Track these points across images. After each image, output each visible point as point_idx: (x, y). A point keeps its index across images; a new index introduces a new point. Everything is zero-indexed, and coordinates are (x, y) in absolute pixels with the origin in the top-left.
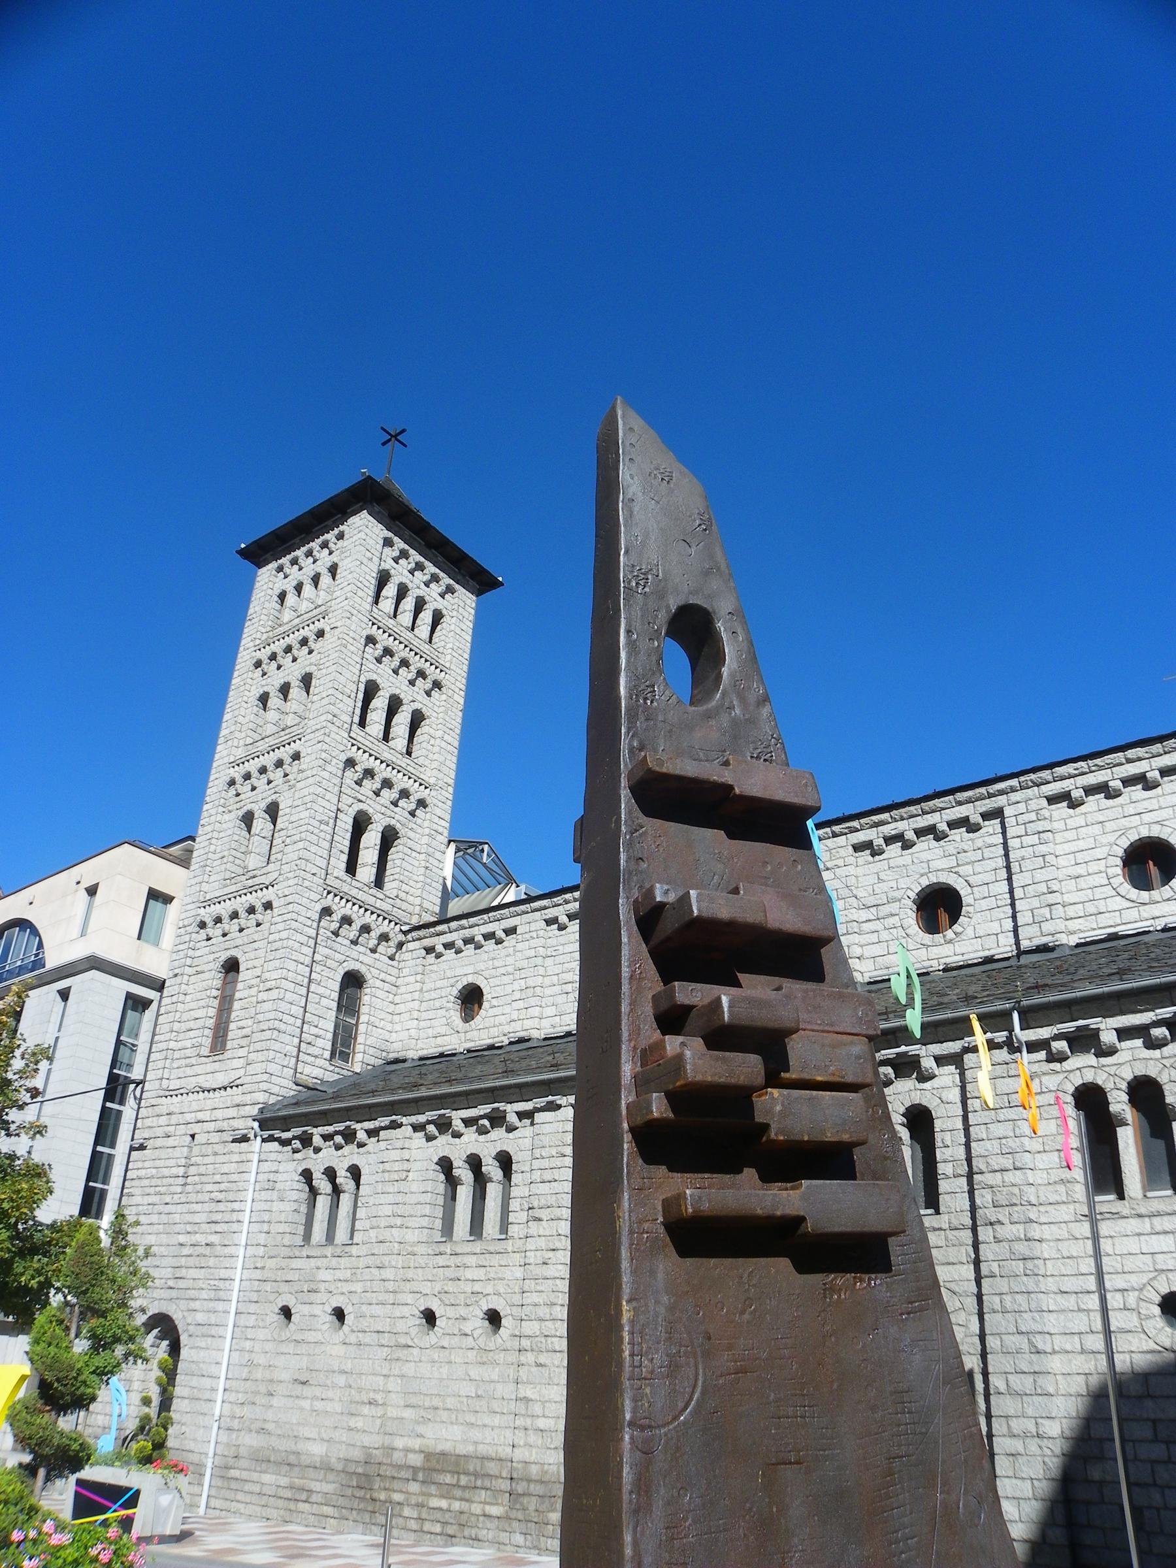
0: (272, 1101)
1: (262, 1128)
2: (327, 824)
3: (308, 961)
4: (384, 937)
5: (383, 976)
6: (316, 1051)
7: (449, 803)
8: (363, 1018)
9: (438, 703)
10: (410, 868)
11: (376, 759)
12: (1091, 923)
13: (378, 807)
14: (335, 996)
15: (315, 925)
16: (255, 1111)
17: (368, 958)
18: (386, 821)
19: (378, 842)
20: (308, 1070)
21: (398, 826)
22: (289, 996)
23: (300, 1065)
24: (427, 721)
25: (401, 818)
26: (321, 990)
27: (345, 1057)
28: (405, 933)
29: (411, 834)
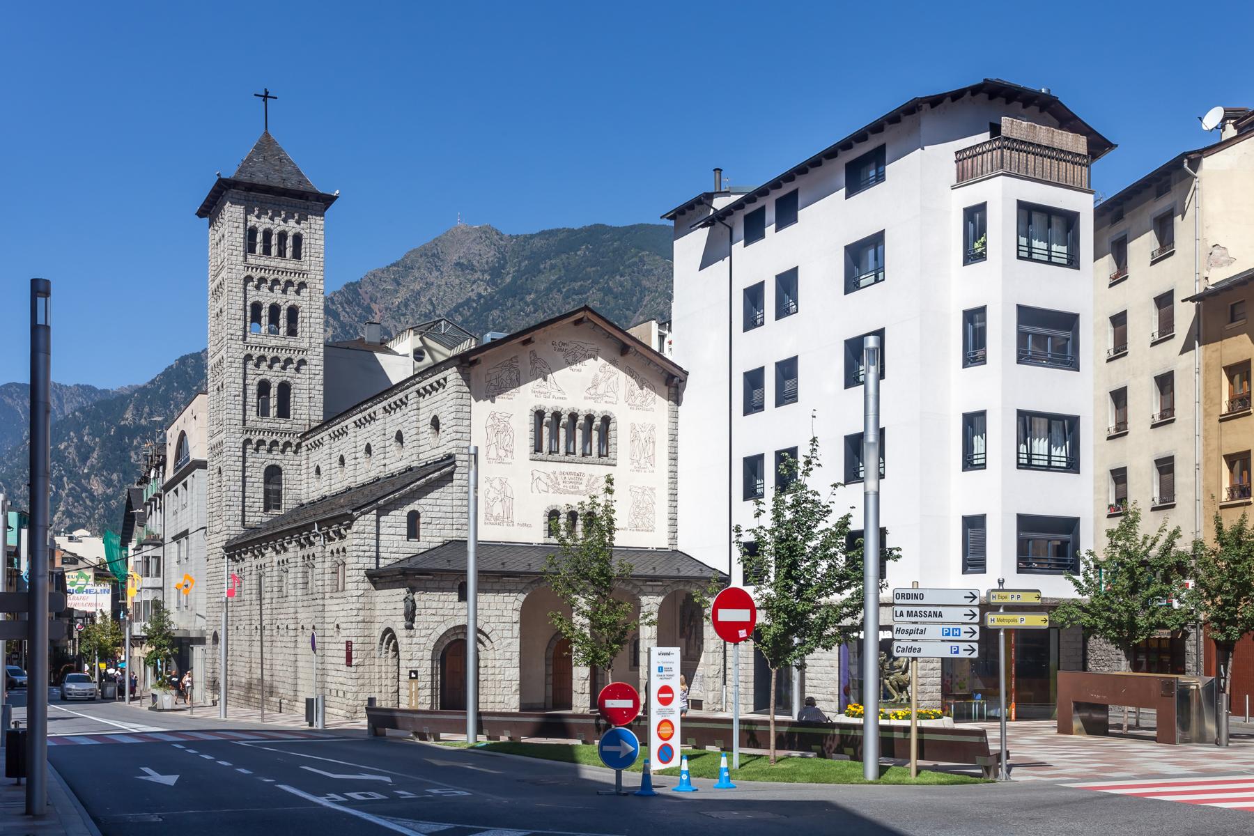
0: (232, 537)
1: (226, 552)
2: (239, 396)
3: (240, 468)
4: (288, 444)
5: (291, 462)
6: (255, 509)
7: (322, 354)
8: (284, 486)
9: (306, 295)
10: (300, 400)
11: (265, 348)
12: (435, 452)
13: (273, 374)
14: (262, 480)
15: (241, 450)
16: (224, 543)
17: (280, 456)
18: (279, 380)
19: (276, 393)
20: (251, 519)
21: (289, 379)
22: (232, 488)
23: (247, 519)
24: (300, 310)
25: (290, 375)
26: (253, 480)
27: (278, 507)
28: (300, 437)
29: (298, 381)
